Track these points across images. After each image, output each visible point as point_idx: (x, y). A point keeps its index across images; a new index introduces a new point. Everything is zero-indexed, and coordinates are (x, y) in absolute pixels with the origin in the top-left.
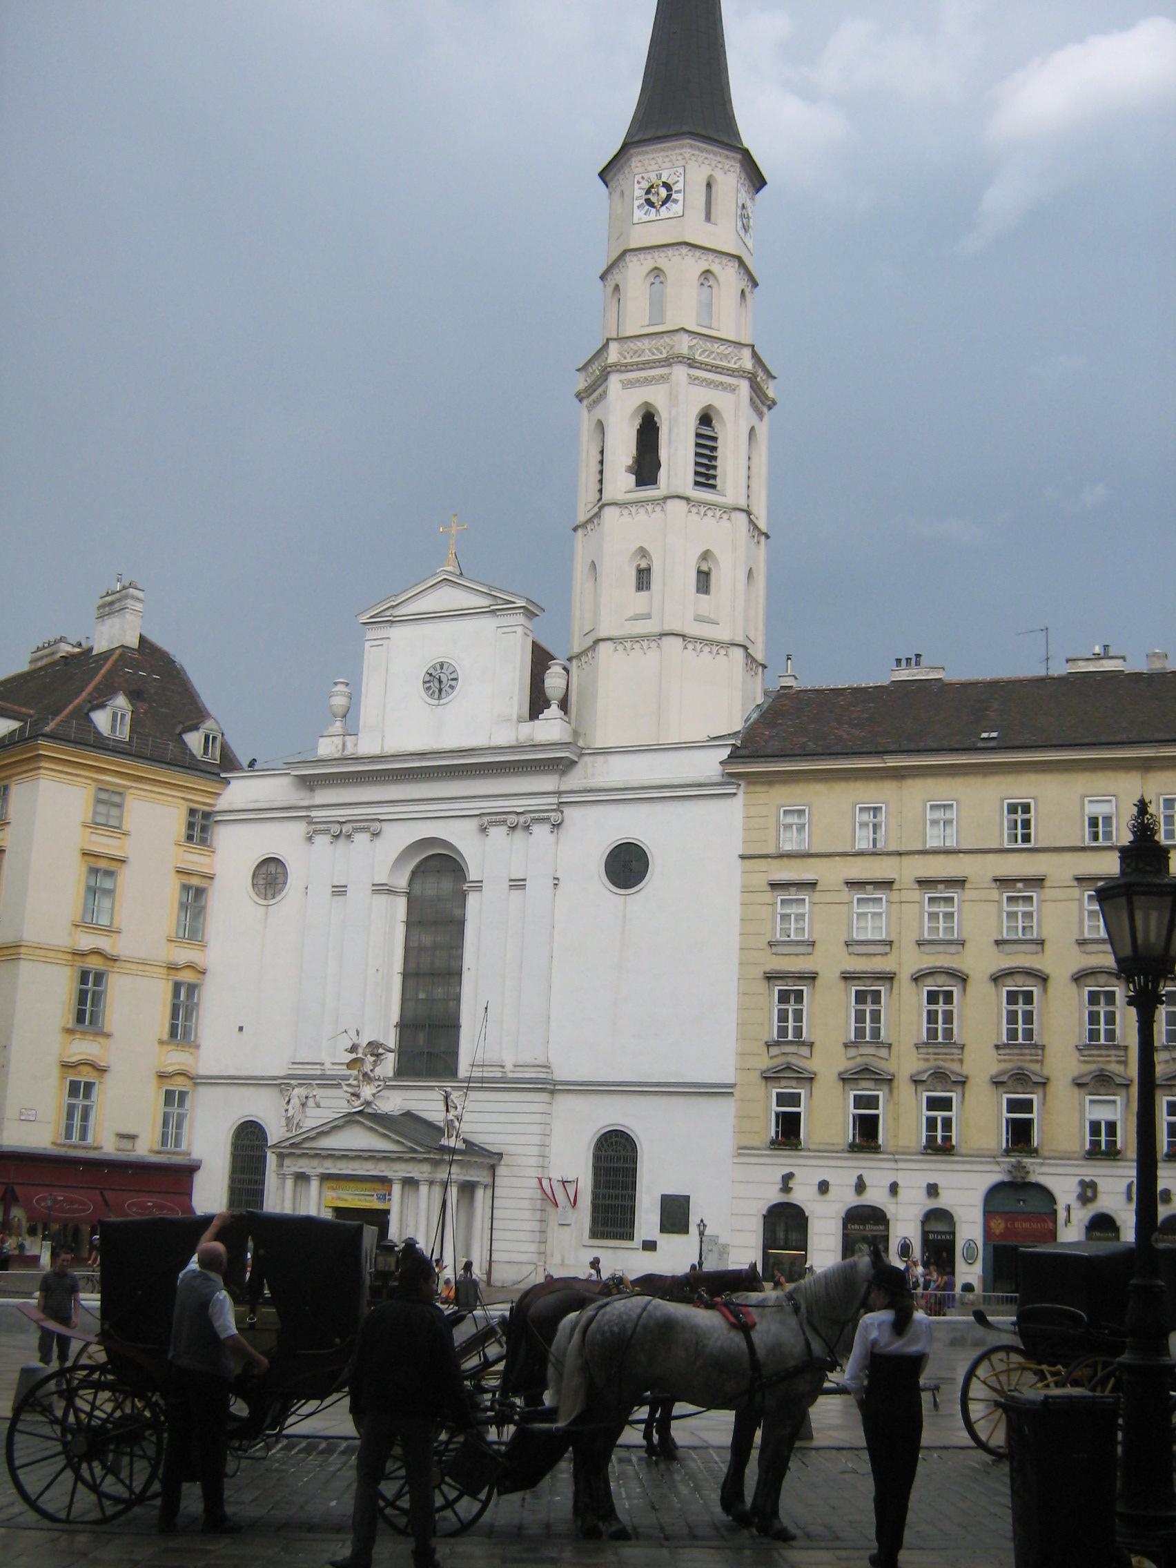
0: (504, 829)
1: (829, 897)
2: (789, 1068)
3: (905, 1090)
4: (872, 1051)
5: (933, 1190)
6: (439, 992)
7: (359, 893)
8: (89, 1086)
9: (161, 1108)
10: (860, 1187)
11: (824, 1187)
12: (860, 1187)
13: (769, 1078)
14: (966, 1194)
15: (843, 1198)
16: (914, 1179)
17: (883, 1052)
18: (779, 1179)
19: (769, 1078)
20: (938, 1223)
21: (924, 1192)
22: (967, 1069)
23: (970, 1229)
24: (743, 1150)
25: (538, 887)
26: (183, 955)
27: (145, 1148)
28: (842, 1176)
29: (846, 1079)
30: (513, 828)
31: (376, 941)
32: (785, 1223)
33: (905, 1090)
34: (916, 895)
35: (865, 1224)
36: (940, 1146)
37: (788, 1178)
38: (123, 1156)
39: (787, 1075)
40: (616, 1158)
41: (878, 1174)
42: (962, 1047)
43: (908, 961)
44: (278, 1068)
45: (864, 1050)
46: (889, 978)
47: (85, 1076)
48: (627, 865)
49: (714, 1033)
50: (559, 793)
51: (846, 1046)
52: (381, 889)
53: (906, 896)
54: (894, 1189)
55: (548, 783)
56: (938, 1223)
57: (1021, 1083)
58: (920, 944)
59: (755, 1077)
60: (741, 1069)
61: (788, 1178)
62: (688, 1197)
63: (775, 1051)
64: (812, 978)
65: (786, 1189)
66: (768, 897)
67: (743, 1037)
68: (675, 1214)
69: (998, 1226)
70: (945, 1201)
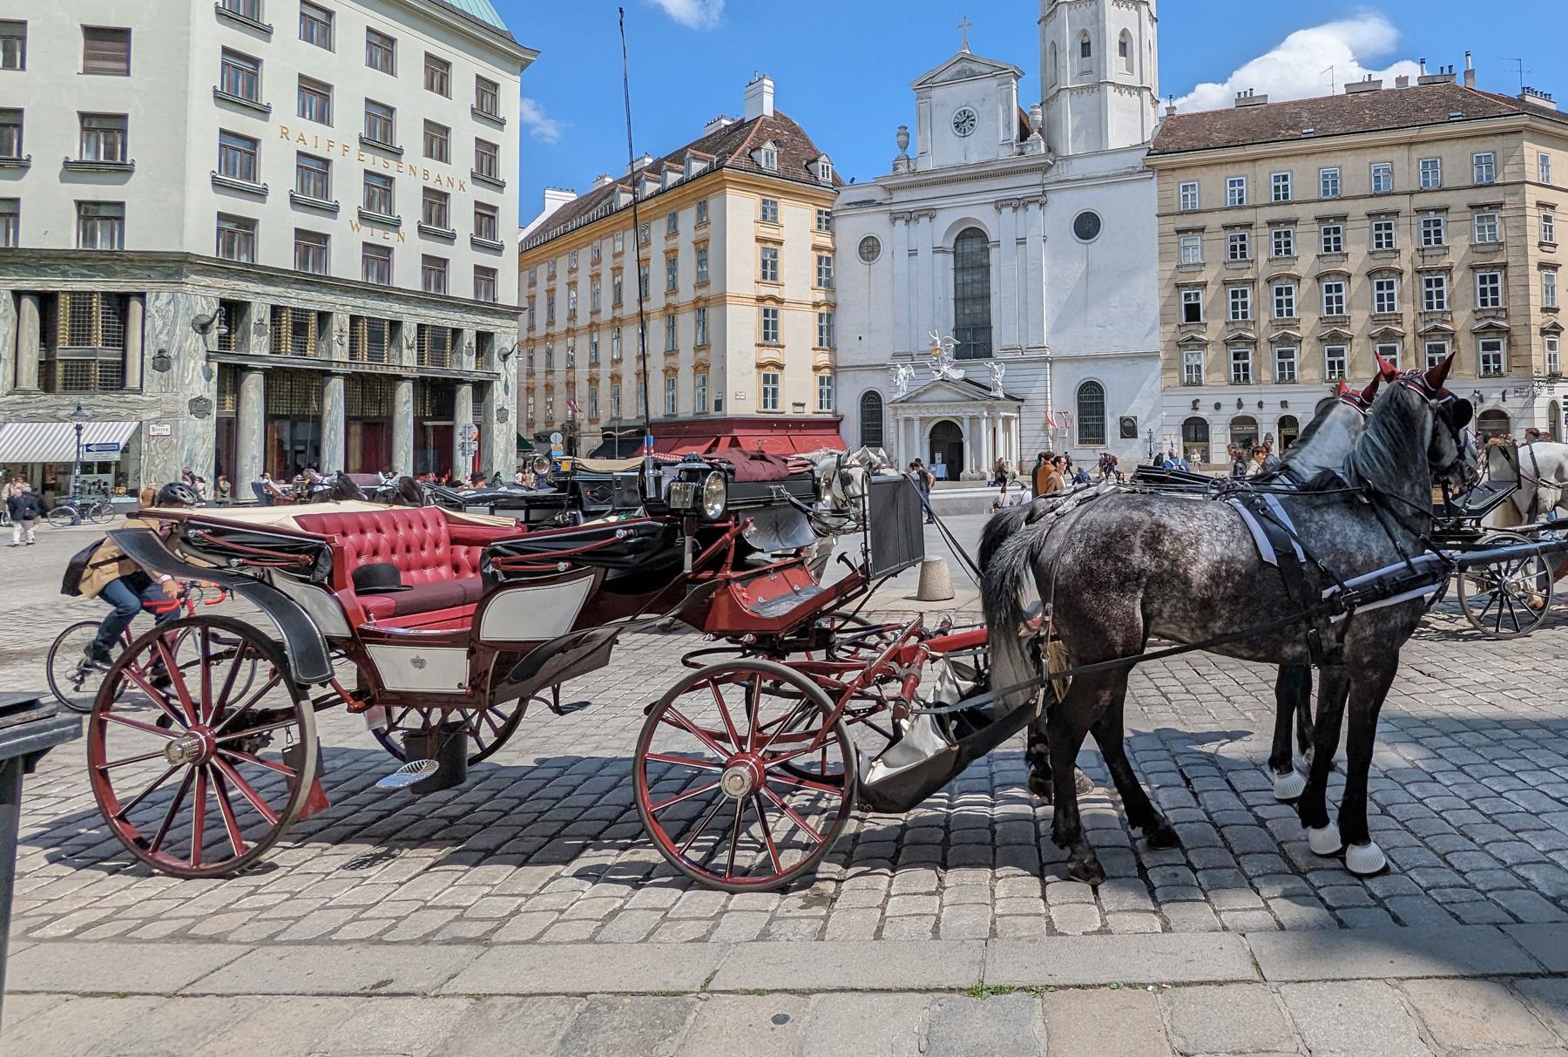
6: (978, 308)
7: (925, 253)
8: (775, 378)
9: (818, 387)
10: (1240, 405)
11: (1218, 406)
12: (1240, 405)
15: (1230, 411)
27: (810, 411)
37: (1195, 402)
38: (798, 416)
40: (1091, 399)
47: (772, 371)
52: (936, 250)
54: (1260, 405)
61: (1195, 402)
65: (1195, 408)
68: (1129, 430)
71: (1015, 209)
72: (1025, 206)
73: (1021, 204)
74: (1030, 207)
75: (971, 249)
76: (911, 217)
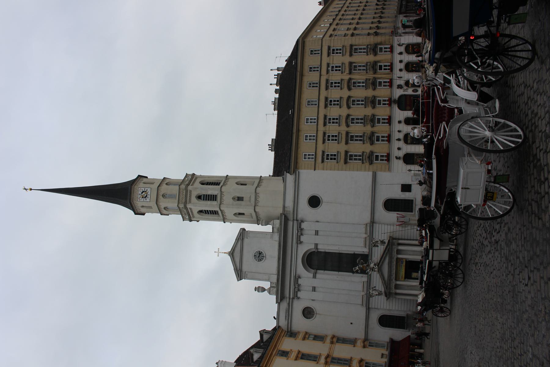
0: (301, 237)
1: (327, 147)
2: (369, 157)
3: (375, 129)
4: (365, 137)
5: (400, 122)
10: (399, 140)
11: (399, 149)
12: (399, 140)
13: (371, 163)
14: (400, 115)
16: (396, 127)
17: (366, 134)
18: (397, 160)
19: (371, 163)
20: (408, 121)
21: (400, 124)
22: (370, 114)
23: (409, 114)
24: (389, 170)
25: (317, 227)
26: (328, 340)
28: (396, 144)
29: (372, 143)
30: (302, 234)
31: (328, 280)
32: (409, 159)
33: (375, 129)
34: (327, 127)
35: (408, 139)
36: (389, 121)
37: (397, 158)
39: (370, 159)
41: (396, 135)
42: (365, 116)
43: (343, 128)
44: (363, 310)
45: (365, 139)
46: (347, 133)
48: (314, 202)
49: (361, 177)
50: (294, 220)
51: (364, 143)
53: (327, 129)
54: (399, 131)
55: (290, 223)
56: (408, 121)
57: (373, 102)
58: (339, 126)
59: (371, 166)
60: (369, 171)
61: (397, 158)
62: (402, 185)
63: (365, 162)
64: (346, 152)
66: (325, 163)
67: (361, 170)
69: (408, 108)
70: (402, 119)
71: (302, 234)
72: (302, 230)
73: (301, 230)
74: (302, 227)
75: (317, 261)
76: (298, 288)
